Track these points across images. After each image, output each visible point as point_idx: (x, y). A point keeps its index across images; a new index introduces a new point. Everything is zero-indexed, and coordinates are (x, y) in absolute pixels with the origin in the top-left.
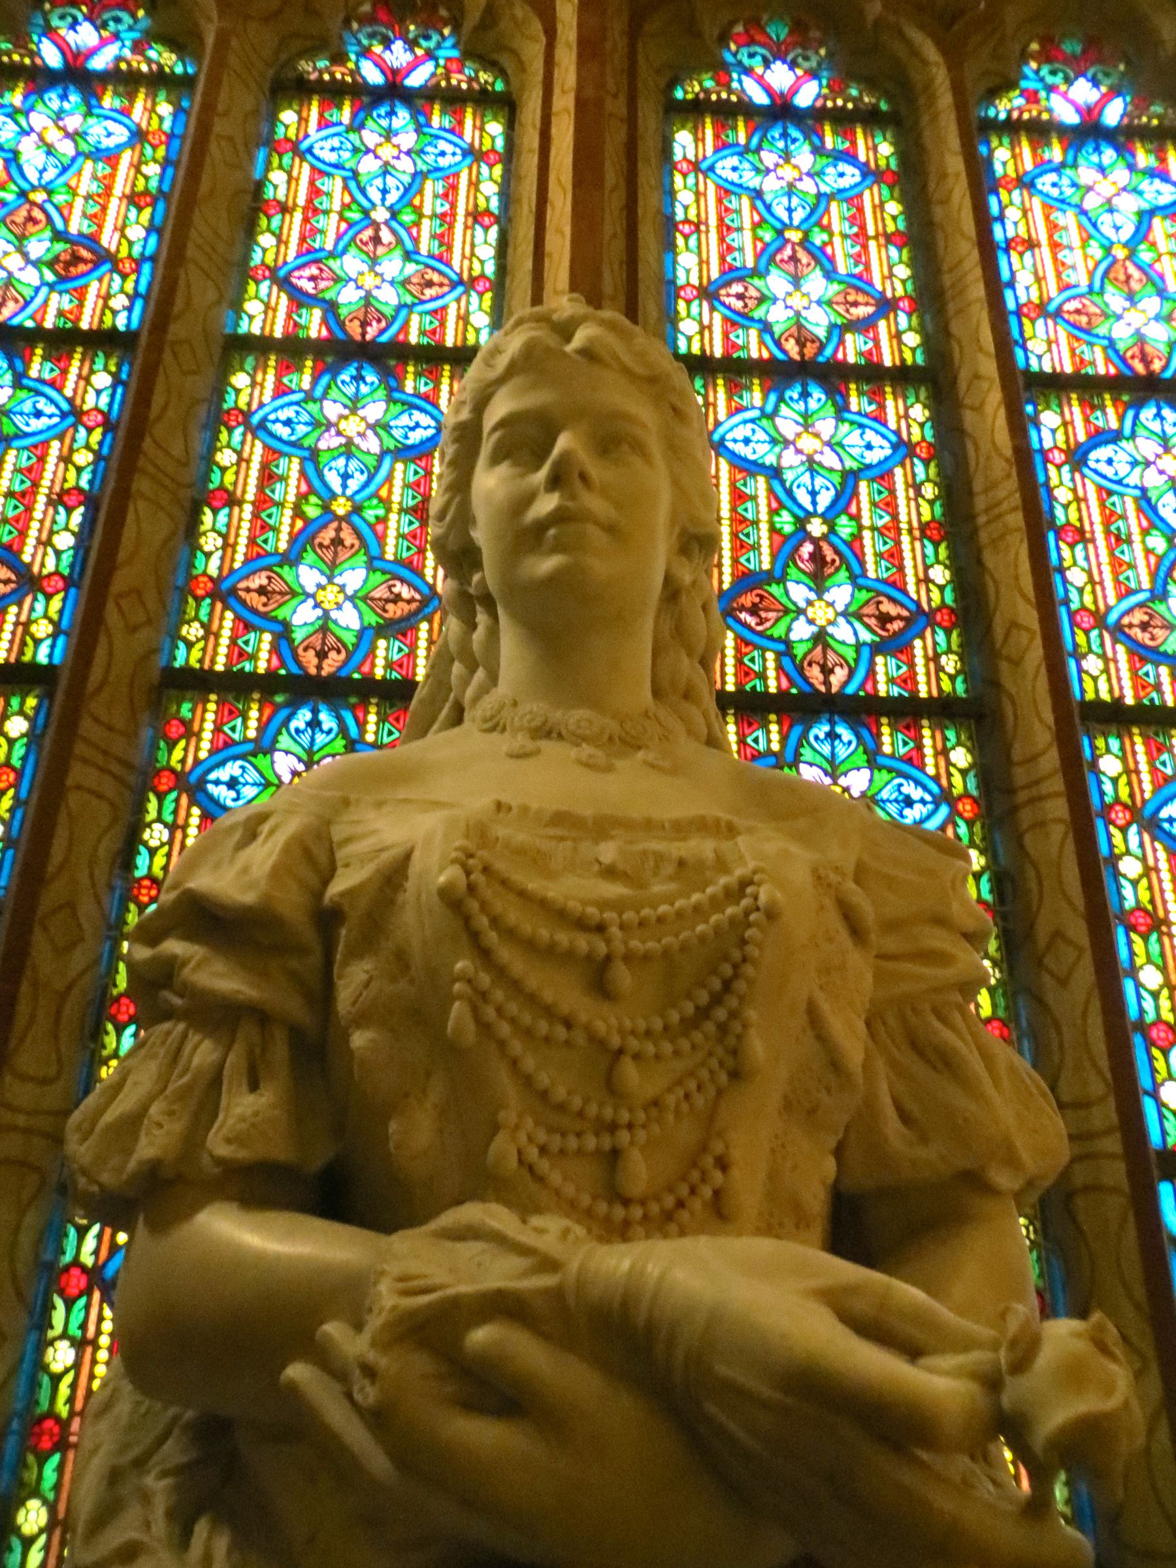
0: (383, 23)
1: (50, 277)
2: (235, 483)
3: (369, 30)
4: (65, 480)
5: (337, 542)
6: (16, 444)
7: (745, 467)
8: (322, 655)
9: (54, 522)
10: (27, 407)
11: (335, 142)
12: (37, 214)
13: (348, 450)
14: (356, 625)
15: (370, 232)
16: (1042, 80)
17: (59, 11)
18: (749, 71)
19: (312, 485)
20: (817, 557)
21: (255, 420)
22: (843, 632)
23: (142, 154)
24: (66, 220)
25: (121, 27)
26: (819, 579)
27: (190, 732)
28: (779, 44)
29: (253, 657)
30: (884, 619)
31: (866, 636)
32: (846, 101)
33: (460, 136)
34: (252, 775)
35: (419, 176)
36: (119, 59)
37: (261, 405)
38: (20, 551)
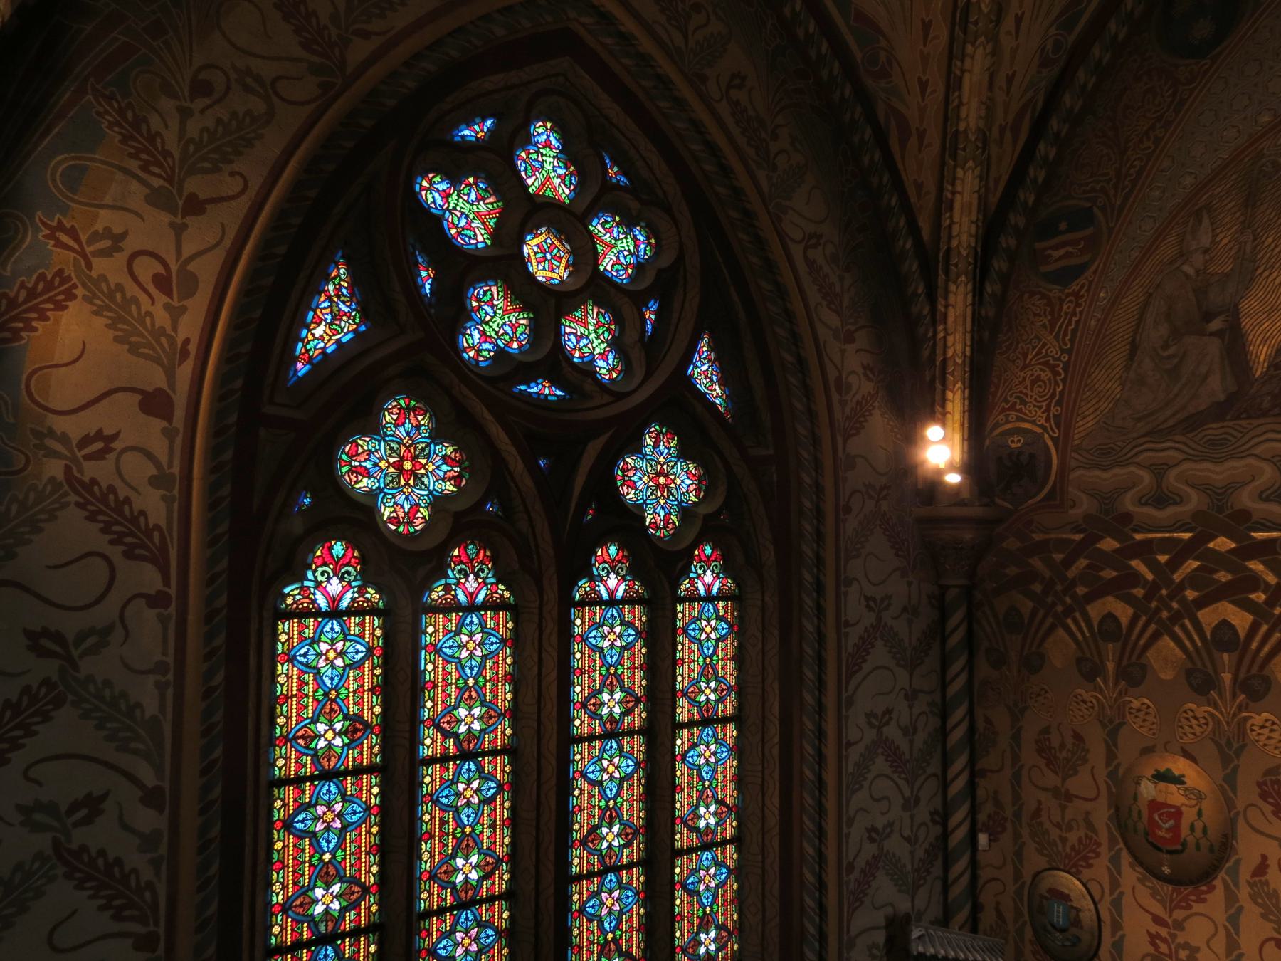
0: (464, 564)
1: (346, 741)
2: (431, 829)
3: (458, 567)
4: (370, 842)
5: (468, 845)
6: (349, 829)
7: (593, 783)
8: (466, 893)
9: (370, 862)
10: (349, 810)
11: (450, 643)
12: (334, 706)
13: (468, 804)
14: (476, 877)
15: (467, 693)
16: (697, 573)
17: (320, 570)
18: (601, 580)
19: (459, 823)
20: (611, 815)
21: (435, 797)
22: (616, 843)
23: (373, 663)
24: (348, 708)
25: (352, 578)
26: (610, 827)
27: (430, 934)
28: (613, 561)
29: (445, 900)
30: (627, 835)
31: (622, 842)
32: (633, 593)
33: (498, 632)
34: (450, 943)
35: (484, 657)
36: (353, 600)
37: (436, 790)
38: (360, 878)
